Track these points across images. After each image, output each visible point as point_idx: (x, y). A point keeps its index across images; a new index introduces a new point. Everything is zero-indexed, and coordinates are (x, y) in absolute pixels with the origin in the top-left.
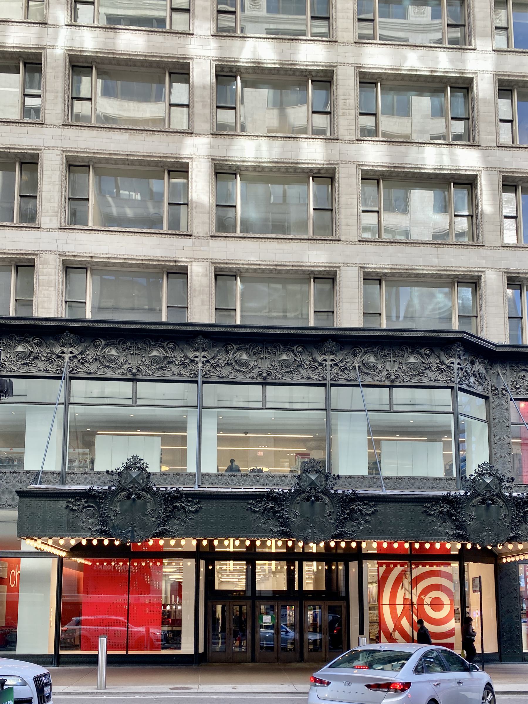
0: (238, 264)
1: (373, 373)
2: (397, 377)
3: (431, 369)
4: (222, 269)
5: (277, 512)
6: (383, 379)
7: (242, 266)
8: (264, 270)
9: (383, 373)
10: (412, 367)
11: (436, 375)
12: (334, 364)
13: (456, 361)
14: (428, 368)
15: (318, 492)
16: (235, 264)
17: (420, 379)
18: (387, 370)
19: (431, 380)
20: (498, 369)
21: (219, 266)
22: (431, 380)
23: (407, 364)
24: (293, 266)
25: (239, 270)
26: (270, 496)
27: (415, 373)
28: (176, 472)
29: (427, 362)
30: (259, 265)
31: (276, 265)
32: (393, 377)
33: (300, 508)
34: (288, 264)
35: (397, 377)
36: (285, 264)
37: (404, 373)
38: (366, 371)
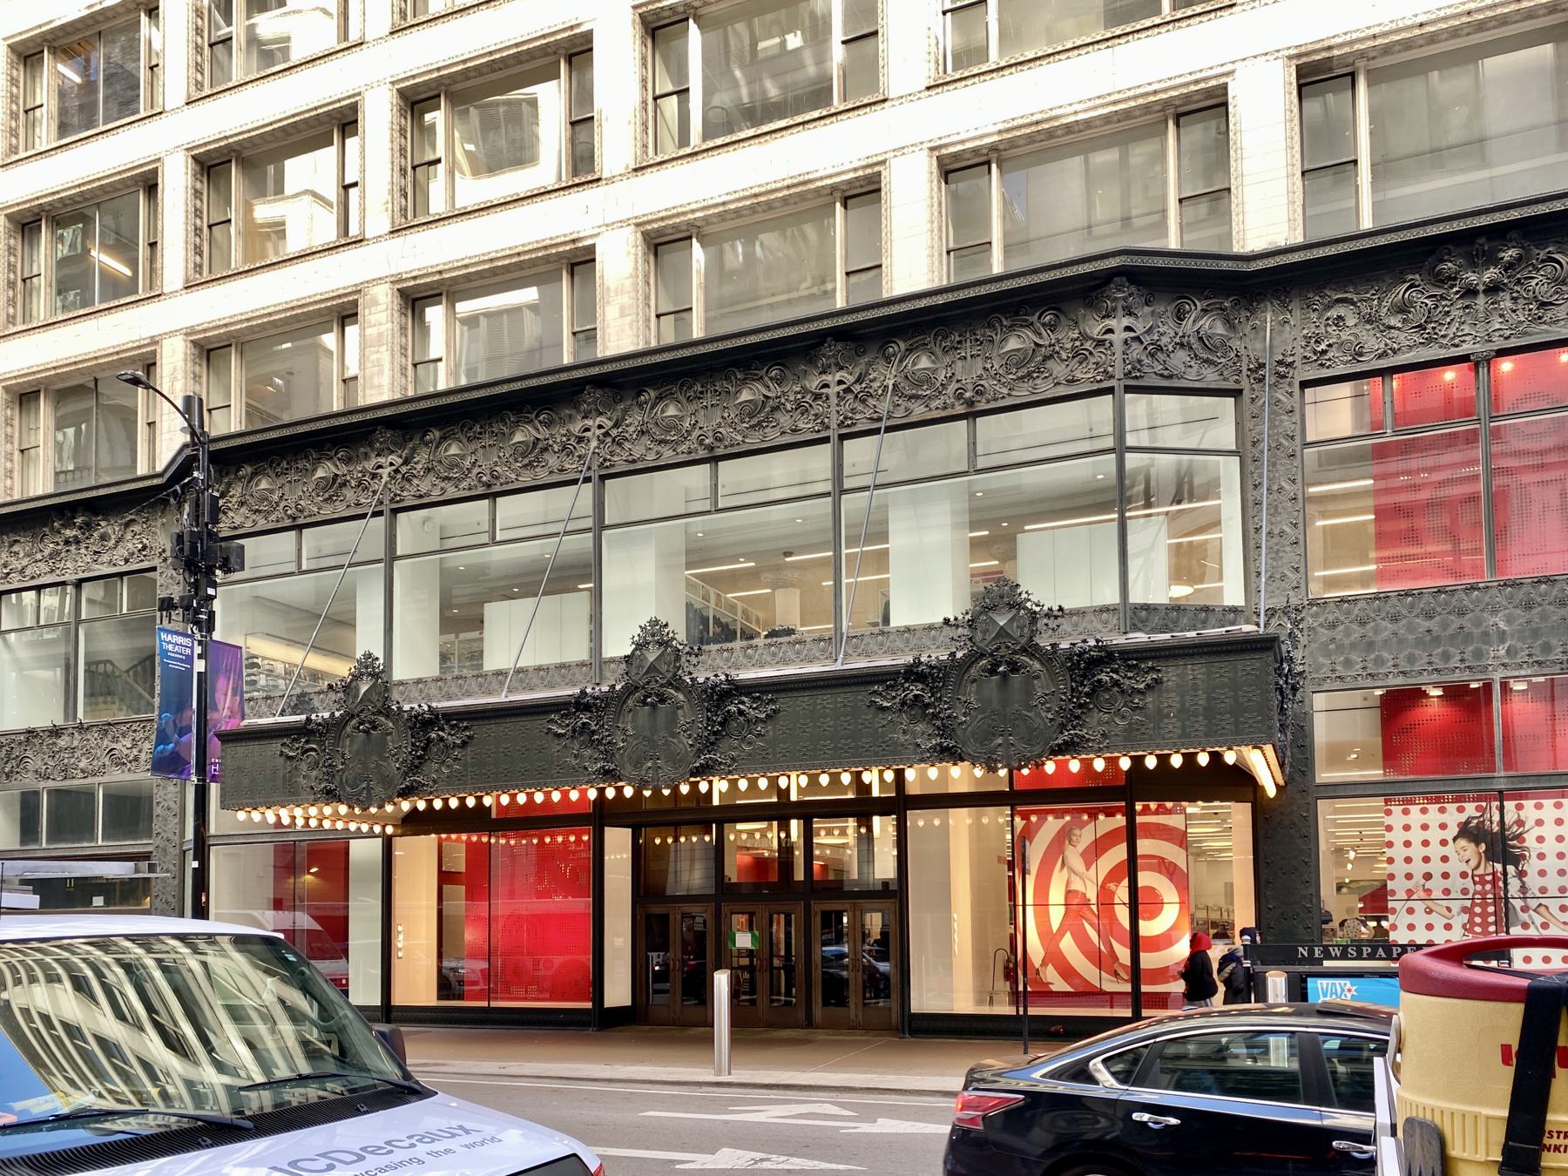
0: (684, 213)
4: (660, 232)
5: (927, 706)
7: (691, 216)
8: (737, 211)
15: (1015, 653)
16: (678, 215)
20: (1269, 317)
21: (649, 227)
24: (788, 187)
25: (690, 224)
26: (913, 673)
28: (816, 636)
30: (724, 204)
31: (756, 195)
33: (977, 693)
34: (779, 185)
36: (774, 186)
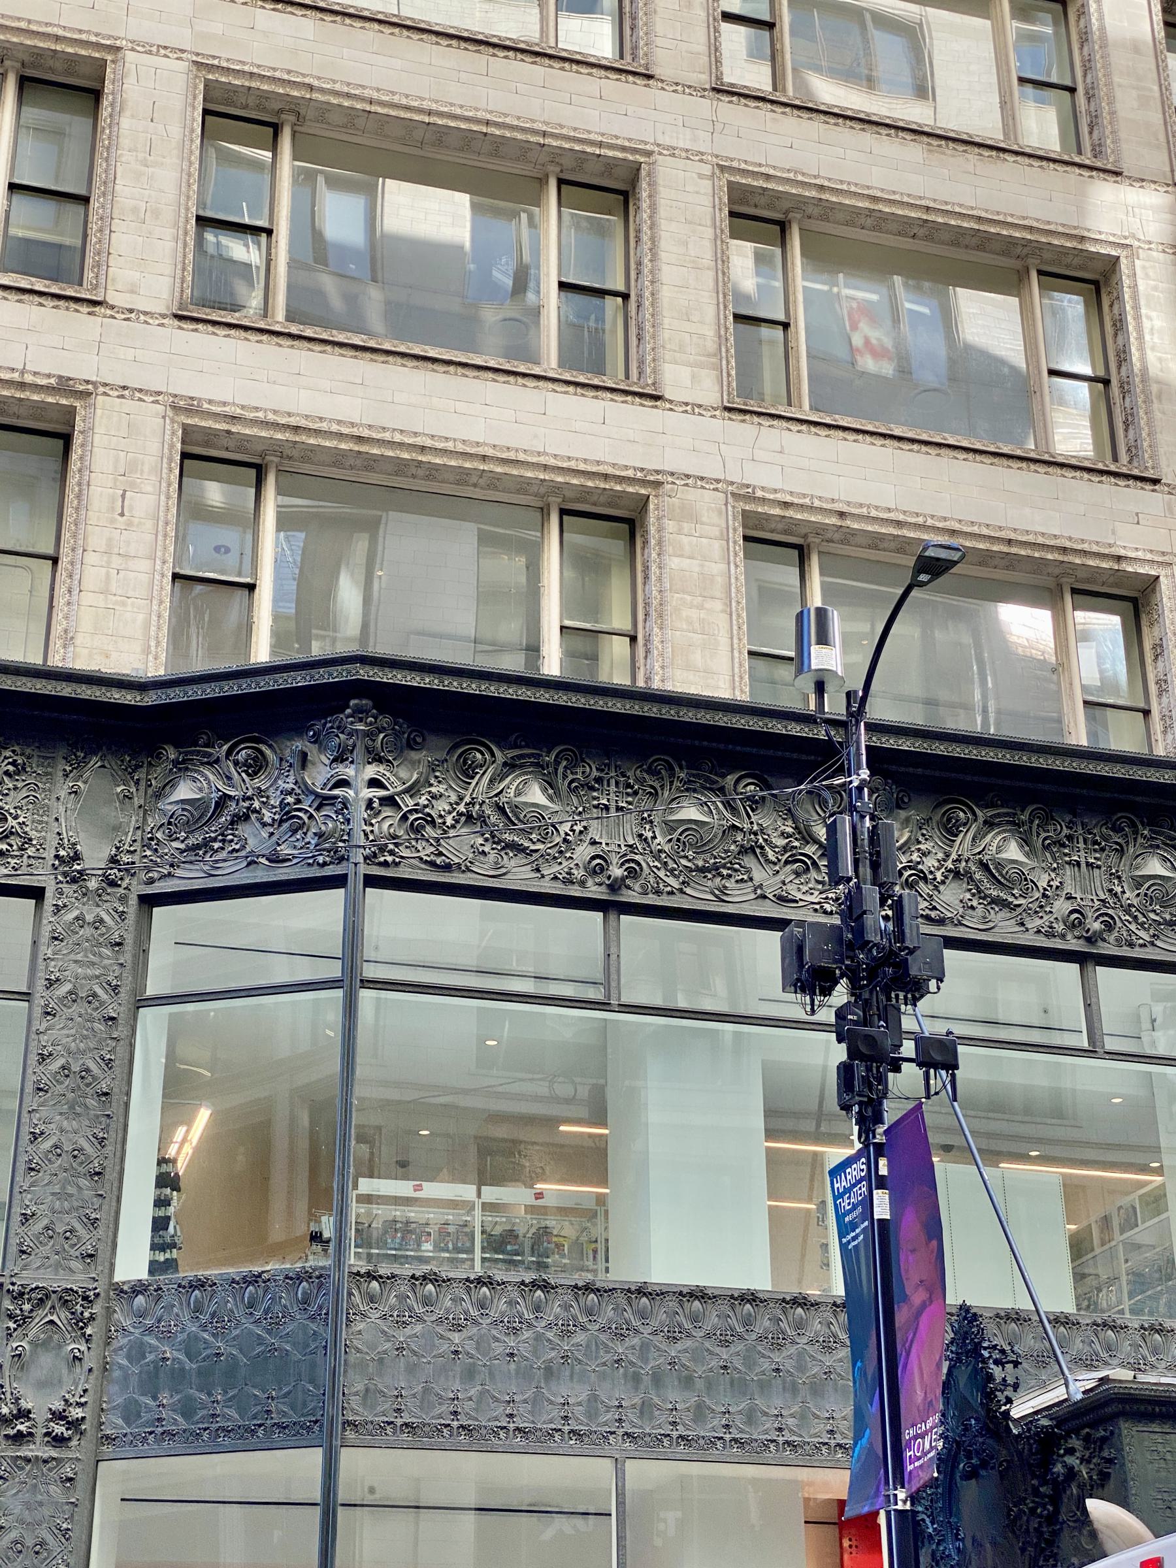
1: (540, 846)
2: (633, 873)
3: (764, 855)
6: (578, 874)
9: (579, 850)
10: (690, 837)
11: (781, 877)
12: (383, 800)
13: (361, 772)
14: (752, 849)
17: (723, 889)
18: (594, 843)
19: (764, 897)
22: (764, 897)
23: (670, 827)
27: (700, 863)
29: (746, 826)
32: (617, 872)
35: (633, 873)
37: (658, 859)
38: (508, 837)
